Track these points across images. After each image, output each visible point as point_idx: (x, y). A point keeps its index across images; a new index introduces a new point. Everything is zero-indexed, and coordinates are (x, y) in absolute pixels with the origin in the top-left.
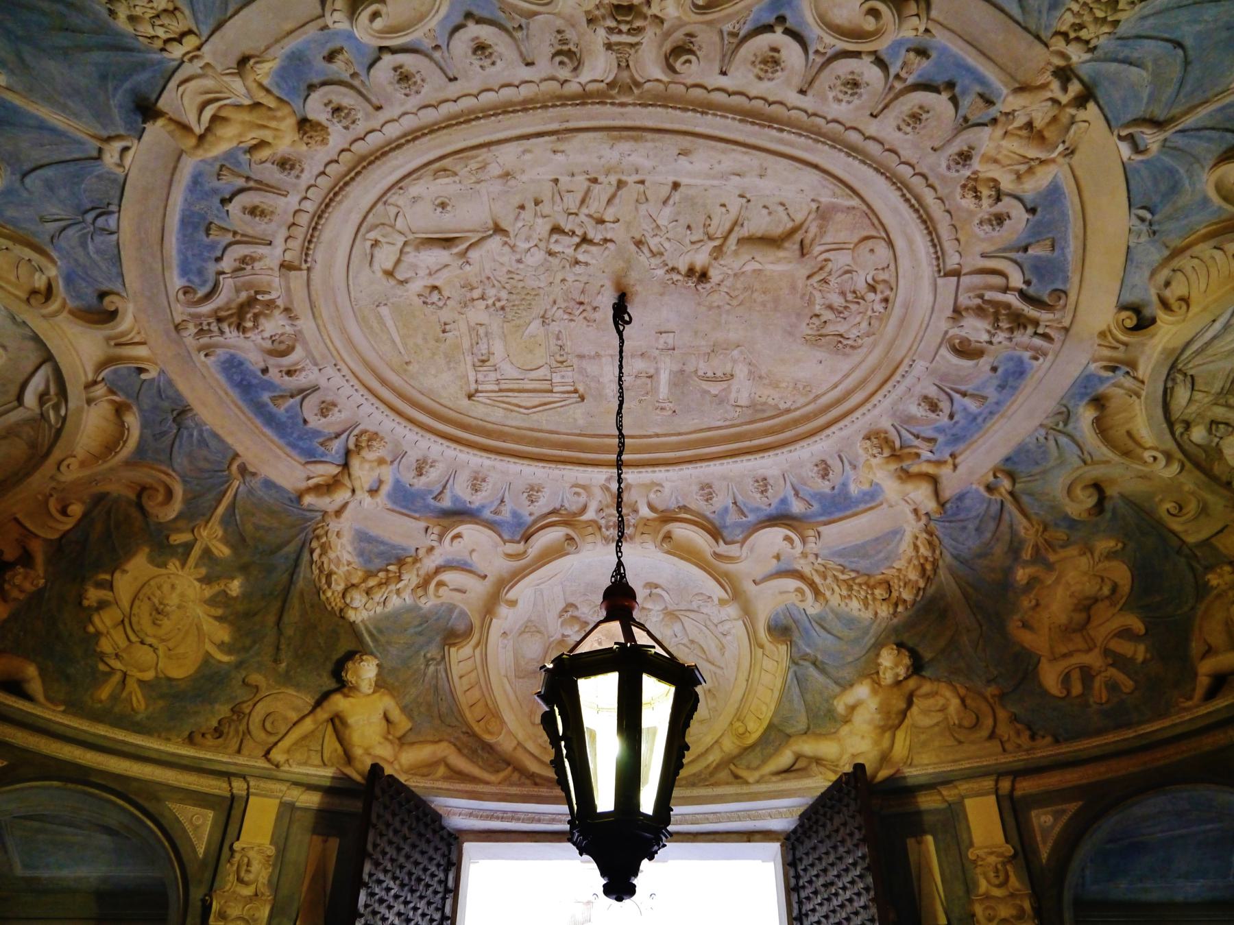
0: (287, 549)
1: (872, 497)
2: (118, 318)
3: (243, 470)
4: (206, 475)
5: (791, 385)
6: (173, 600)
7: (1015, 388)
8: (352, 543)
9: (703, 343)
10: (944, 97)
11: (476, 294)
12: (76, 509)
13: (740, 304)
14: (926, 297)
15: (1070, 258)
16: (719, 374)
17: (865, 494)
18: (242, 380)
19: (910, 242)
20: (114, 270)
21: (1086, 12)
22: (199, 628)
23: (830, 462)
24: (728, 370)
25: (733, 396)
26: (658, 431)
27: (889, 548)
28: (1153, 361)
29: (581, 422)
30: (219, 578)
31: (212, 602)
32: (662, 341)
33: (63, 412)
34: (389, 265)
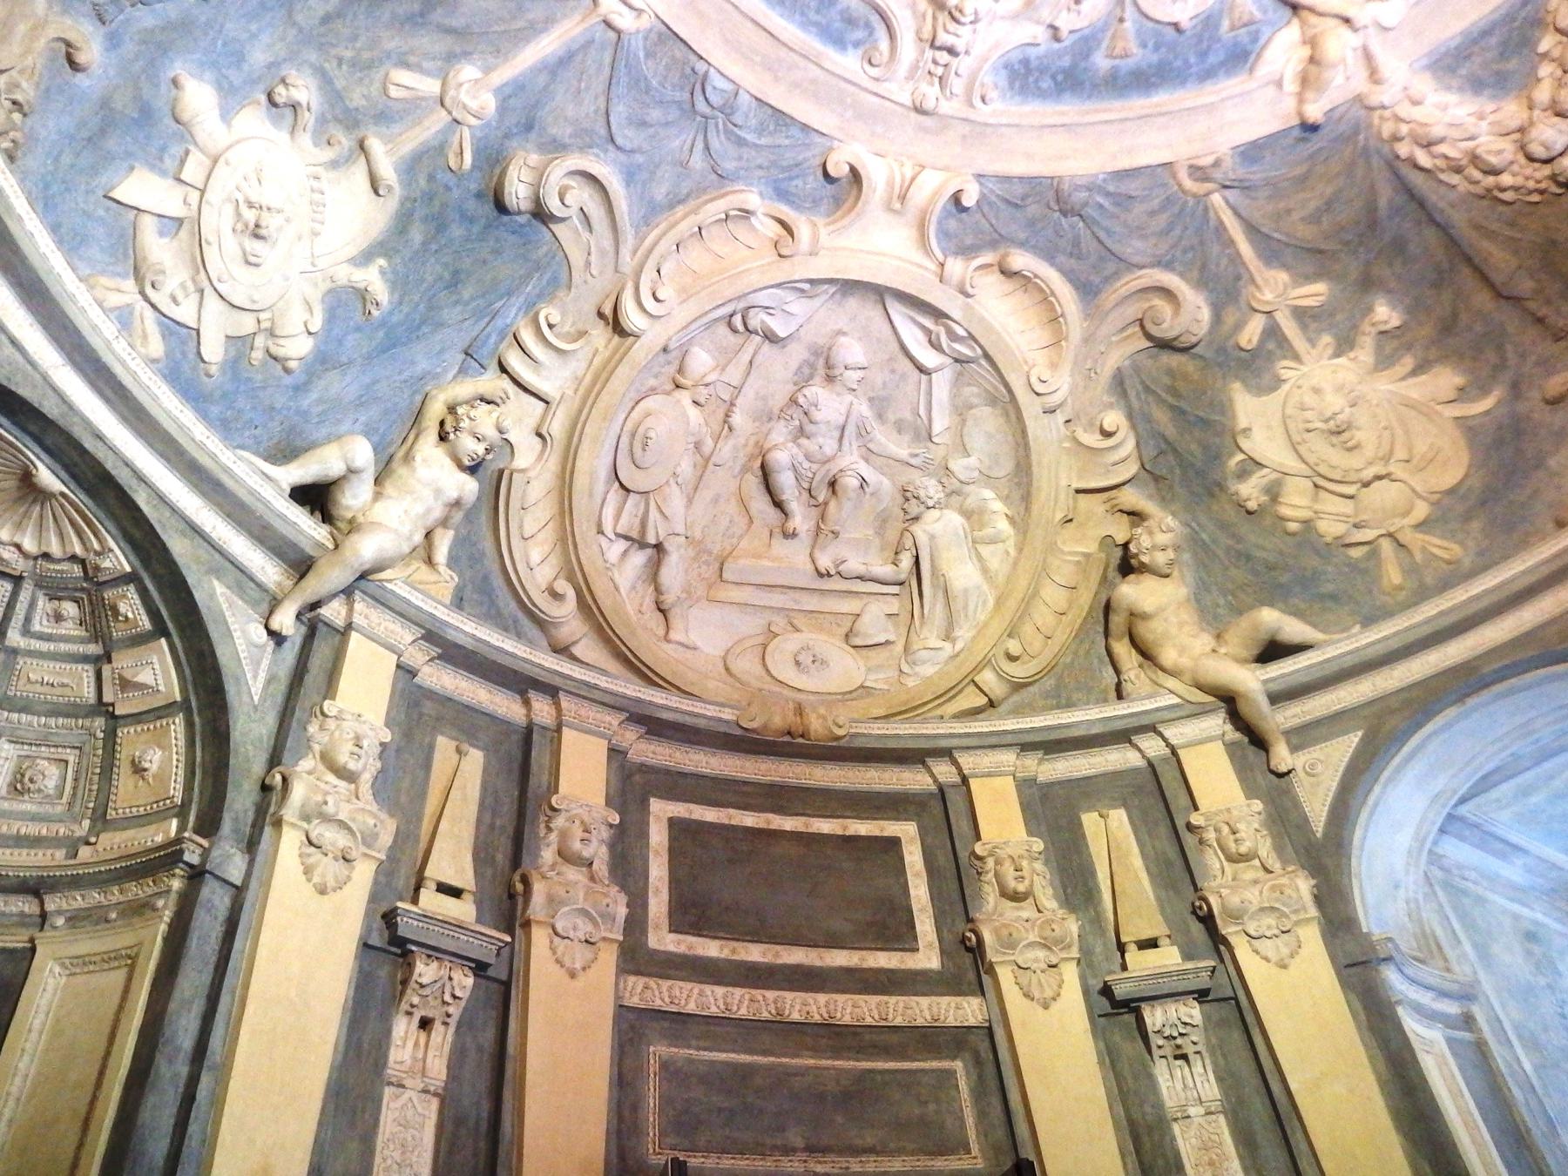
0: (1383, 202)
2: (862, 172)
4: (1177, 232)
6: (1335, 403)
8: (1448, 88)
12: (1114, 418)
18: (1053, 77)
20: (795, 131)
22: (1410, 405)
30: (1355, 327)
31: (1384, 362)
33: (961, 332)
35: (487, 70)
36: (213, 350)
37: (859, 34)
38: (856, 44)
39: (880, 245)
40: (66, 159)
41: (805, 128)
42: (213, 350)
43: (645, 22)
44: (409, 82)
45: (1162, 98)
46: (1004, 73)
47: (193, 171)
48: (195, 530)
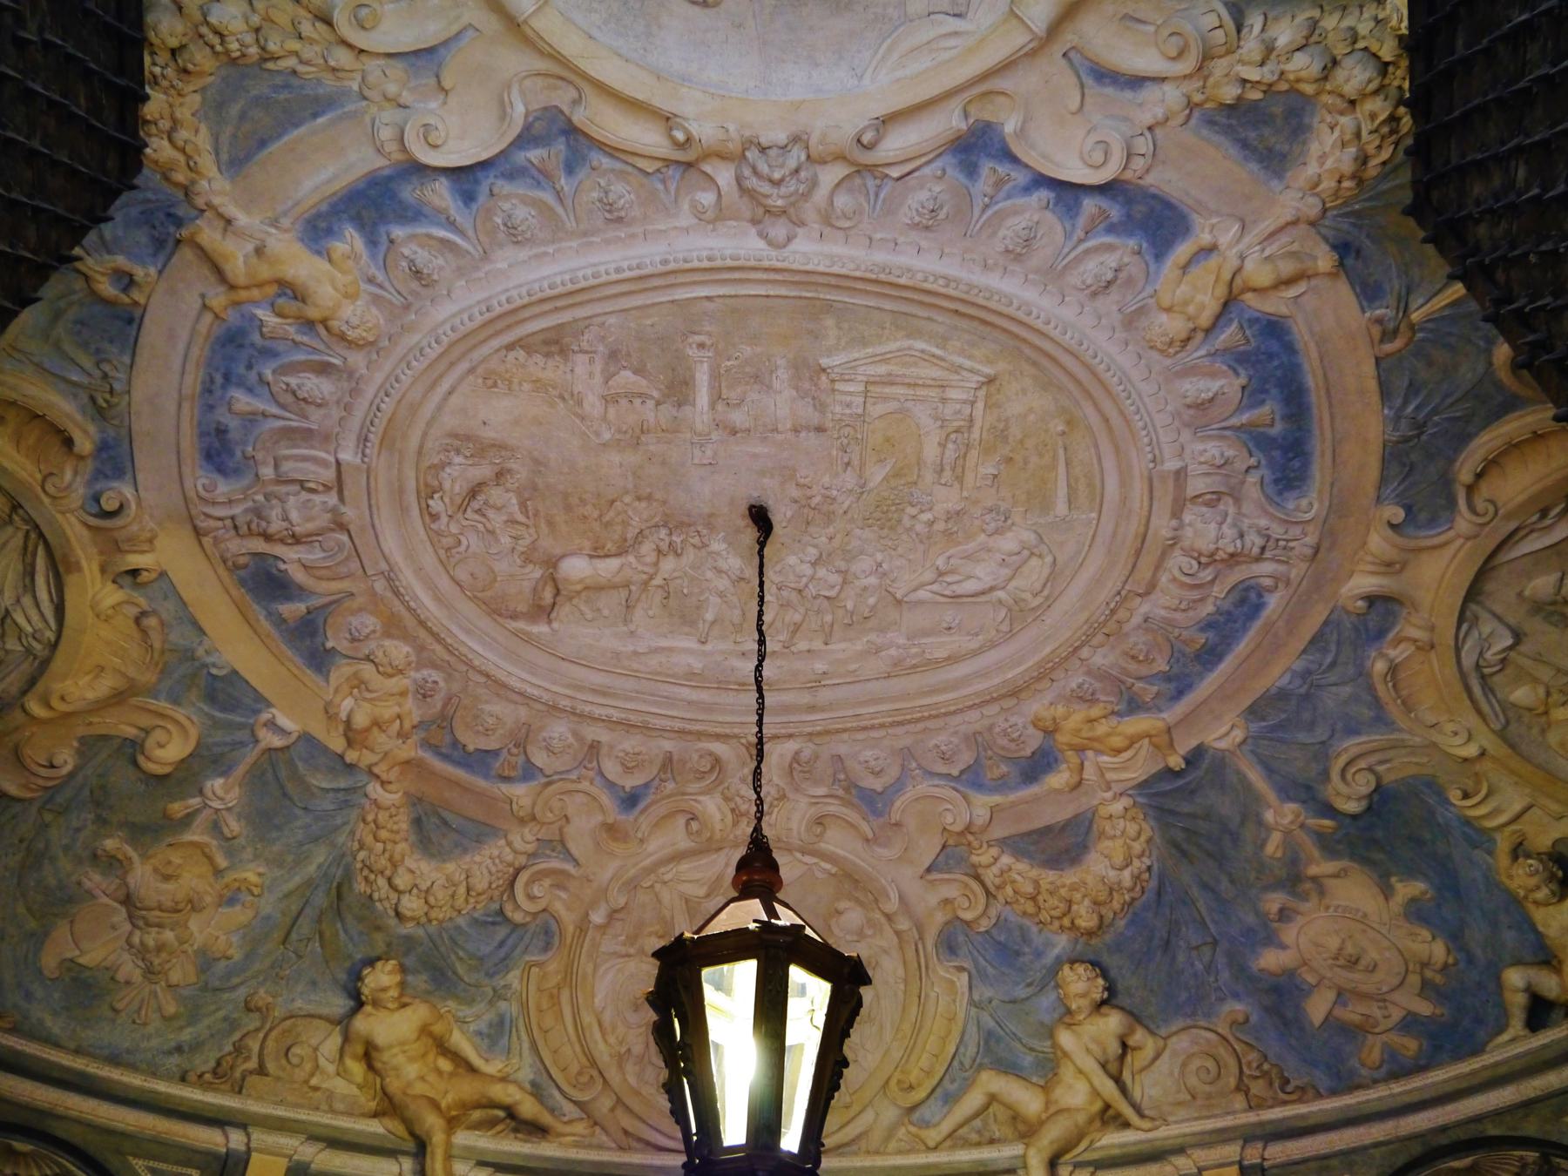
1: (318, 230)
3: (1388, 335)
5: (515, 386)
7: (203, 434)
9: (652, 448)
10: (471, 748)
11: (940, 526)
13: (613, 502)
14: (390, 543)
15: (255, 606)
16: (624, 402)
17: (329, 232)
19: (438, 598)
21: (395, 827)
23: (414, 285)
24: (612, 411)
25: (598, 367)
26: (707, 304)
27: (227, 131)
29: (829, 322)
32: (709, 453)
34: (1034, 562)
37: (1253, 595)
38: (1260, 596)
39: (1438, 573)
40: (1293, 1042)
41: (1326, 623)
42: (1425, 1008)
44: (1273, 846)
45: (1311, 381)
46: (1286, 494)
47: (1311, 979)
48: (1527, 1105)
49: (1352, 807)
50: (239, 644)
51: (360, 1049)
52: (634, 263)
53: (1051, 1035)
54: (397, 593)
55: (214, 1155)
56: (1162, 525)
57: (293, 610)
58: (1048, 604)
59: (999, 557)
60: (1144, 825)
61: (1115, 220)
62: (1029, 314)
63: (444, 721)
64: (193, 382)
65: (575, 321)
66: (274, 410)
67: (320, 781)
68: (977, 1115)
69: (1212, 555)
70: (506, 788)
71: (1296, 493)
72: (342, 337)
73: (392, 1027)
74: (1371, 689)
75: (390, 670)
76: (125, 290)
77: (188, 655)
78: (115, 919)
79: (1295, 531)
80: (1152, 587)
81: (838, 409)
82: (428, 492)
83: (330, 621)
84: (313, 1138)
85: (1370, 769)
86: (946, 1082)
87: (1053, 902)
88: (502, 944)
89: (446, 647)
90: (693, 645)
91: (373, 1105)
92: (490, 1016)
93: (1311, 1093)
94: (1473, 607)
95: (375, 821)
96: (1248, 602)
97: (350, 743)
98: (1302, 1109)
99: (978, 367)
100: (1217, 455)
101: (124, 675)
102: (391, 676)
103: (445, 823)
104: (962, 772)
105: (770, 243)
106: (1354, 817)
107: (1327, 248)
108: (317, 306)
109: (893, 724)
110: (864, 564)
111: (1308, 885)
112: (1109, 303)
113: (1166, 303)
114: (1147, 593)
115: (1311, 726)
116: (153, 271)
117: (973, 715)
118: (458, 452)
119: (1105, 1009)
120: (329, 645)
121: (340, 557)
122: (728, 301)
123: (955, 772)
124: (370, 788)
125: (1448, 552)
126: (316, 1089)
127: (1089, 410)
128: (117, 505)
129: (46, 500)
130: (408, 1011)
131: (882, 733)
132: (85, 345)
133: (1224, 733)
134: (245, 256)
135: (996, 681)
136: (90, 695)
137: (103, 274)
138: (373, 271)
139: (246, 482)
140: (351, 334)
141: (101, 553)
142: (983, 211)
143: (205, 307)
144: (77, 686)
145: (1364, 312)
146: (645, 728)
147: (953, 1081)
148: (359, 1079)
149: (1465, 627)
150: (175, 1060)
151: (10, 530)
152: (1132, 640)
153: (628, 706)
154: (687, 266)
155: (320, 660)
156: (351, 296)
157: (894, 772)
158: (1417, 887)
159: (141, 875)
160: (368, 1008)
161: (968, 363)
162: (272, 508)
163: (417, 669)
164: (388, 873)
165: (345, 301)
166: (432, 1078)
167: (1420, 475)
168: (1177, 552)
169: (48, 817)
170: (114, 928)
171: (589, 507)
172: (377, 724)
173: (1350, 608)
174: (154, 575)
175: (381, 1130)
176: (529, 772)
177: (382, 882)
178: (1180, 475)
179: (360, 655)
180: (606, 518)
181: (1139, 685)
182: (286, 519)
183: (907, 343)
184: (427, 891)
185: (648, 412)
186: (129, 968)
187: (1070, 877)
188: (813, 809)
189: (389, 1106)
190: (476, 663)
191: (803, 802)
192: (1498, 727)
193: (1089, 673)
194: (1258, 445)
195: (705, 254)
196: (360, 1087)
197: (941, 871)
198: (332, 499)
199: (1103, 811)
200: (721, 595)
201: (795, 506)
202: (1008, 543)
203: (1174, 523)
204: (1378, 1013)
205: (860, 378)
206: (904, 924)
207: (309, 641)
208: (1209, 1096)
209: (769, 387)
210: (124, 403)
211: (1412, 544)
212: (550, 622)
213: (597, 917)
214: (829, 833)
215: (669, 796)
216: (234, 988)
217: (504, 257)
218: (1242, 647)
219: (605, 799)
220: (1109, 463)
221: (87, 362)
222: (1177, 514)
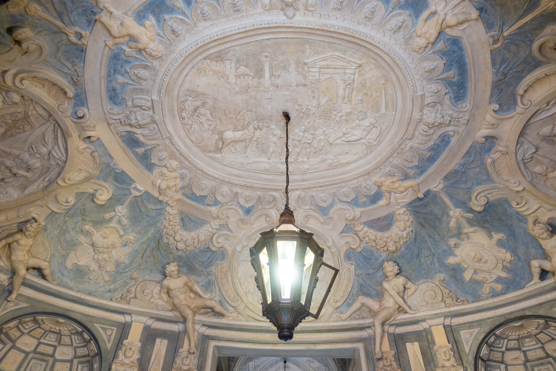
3: (495, 42)
5: (207, 73)
7: (108, 91)
9: (252, 93)
10: (198, 195)
11: (344, 118)
14: (170, 127)
16: (242, 77)
17: (144, 17)
19: (186, 146)
20: (471, 149)
23: (173, 36)
25: (233, 65)
26: (268, 42)
28: (70, 128)
32: (270, 94)
34: (374, 129)
35: (451, 210)
36: (504, 275)
37: (446, 138)
38: (449, 138)
39: (509, 128)
41: (470, 147)
42: (504, 275)
43: (442, 182)
44: (452, 223)
45: (468, 60)
48: (540, 305)
49: (479, 209)
50: (124, 161)
51: (166, 291)
52: (243, 26)
53: (381, 285)
54: (173, 144)
55: (121, 323)
56: (416, 115)
57: (140, 150)
58: (379, 143)
59: (363, 128)
60: (410, 217)
61: (402, 3)
62: (373, 40)
63: (189, 186)
64: (104, 72)
65: (225, 49)
66: (131, 82)
67: (151, 206)
68: (358, 310)
69: (433, 124)
70: (209, 208)
71: (461, 102)
72: (151, 55)
73: (175, 283)
74: (486, 169)
75: (171, 170)
76: (80, 39)
77: (108, 166)
78: (89, 251)
79: (461, 115)
80: (413, 136)
81: (311, 78)
82: (181, 110)
83: (152, 154)
84: (151, 318)
85: (485, 196)
86: (348, 300)
87: (381, 242)
88: (209, 258)
89: (189, 162)
90: (266, 160)
91: (170, 308)
92: (206, 280)
93: (466, 302)
94: (521, 138)
95: (169, 219)
96: (445, 140)
97: (160, 194)
98: (464, 307)
99: (356, 61)
100: (435, 89)
101: (88, 172)
102: (172, 172)
103: (191, 219)
104: (352, 200)
105: (287, 17)
106: (480, 212)
107: (475, 10)
108: (142, 43)
109: (329, 185)
110: (319, 132)
111: (464, 236)
112: (400, 35)
113: (419, 34)
114: (411, 139)
115: (466, 181)
116: (88, 32)
117: (355, 181)
118: (190, 96)
119: (398, 276)
120: (152, 162)
121: (154, 132)
122: (274, 40)
123: (349, 201)
124: (167, 209)
125: (514, 120)
126: (152, 303)
127: (393, 76)
128: (82, 115)
129: (59, 113)
130: (181, 278)
131: (326, 188)
132: (68, 59)
133: (437, 185)
134: (118, 26)
135: (362, 170)
136: (78, 179)
137: (72, 33)
138: (159, 31)
139: (123, 107)
140: (154, 53)
141: (79, 131)
142: (358, 3)
143: (106, 45)
144: (74, 175)
145: (487, 33)
146: (252, 188)
147: (350, 300)
148: (166, 300)
149: (519, 146)
150: (109, 294)
151: (49, 124)
152: (406, 155)
153: (246, 180)
154: (261, 27)
155: (150, 167)
156: (153, 40)
157: (330, 201)
158: (500, 236)
159: (97, 237)
160: (168, 278)
161: (353, 60)
162: (132, 115)
163: (180, 170)
164: (173, 235)
165: (151, 42)
166: (188, 299)
167: (505, 93)
168: (421, 124)
169: (67, 219)
170: (89, 253)
171: (232, 114)
172: (168, 187)
173: (479, 141)
174: (96, 139)
175: (173, 315)
176: (216, 203)
177: (171, 238)
178: (423, 96)
179: (162, 165)
180: (238, 118)
181: (408, 170)
182: (136, 119)
183: (333, 53)
184: (186, 241)
185: (250, 81)
186: (94, 266)
187: (386, 234)
188: (304, 213)
189: (175, 308)
190: (199, 167)
191: (302, 211)
192: (530, 180)
193: (392, 167)
194: (449, 85)
195: (266, 22)
196: (166, 302)
197: (345, 233)
198: (151, 113)
199: (397, 212)
200: (275, 143)
201: (297, 112)
202: (366, 123)
203: (421, 113)
204: (488, 277)
205: (318, 66)
206: (334, 250)
207: (146, 161)
208: (433, 303)
209: (288, 71)
210: (82, 80)
211: (501, 117)
212: (221, 153)
213: (238, 249)
214: (310, 221)
215: (260, 210)
216: (127, 272)
217: (202, 25)
218: (443, 156)
219: (240, 211)
220: (399, 94)
221: (70, 66)
222: (421, 111)
